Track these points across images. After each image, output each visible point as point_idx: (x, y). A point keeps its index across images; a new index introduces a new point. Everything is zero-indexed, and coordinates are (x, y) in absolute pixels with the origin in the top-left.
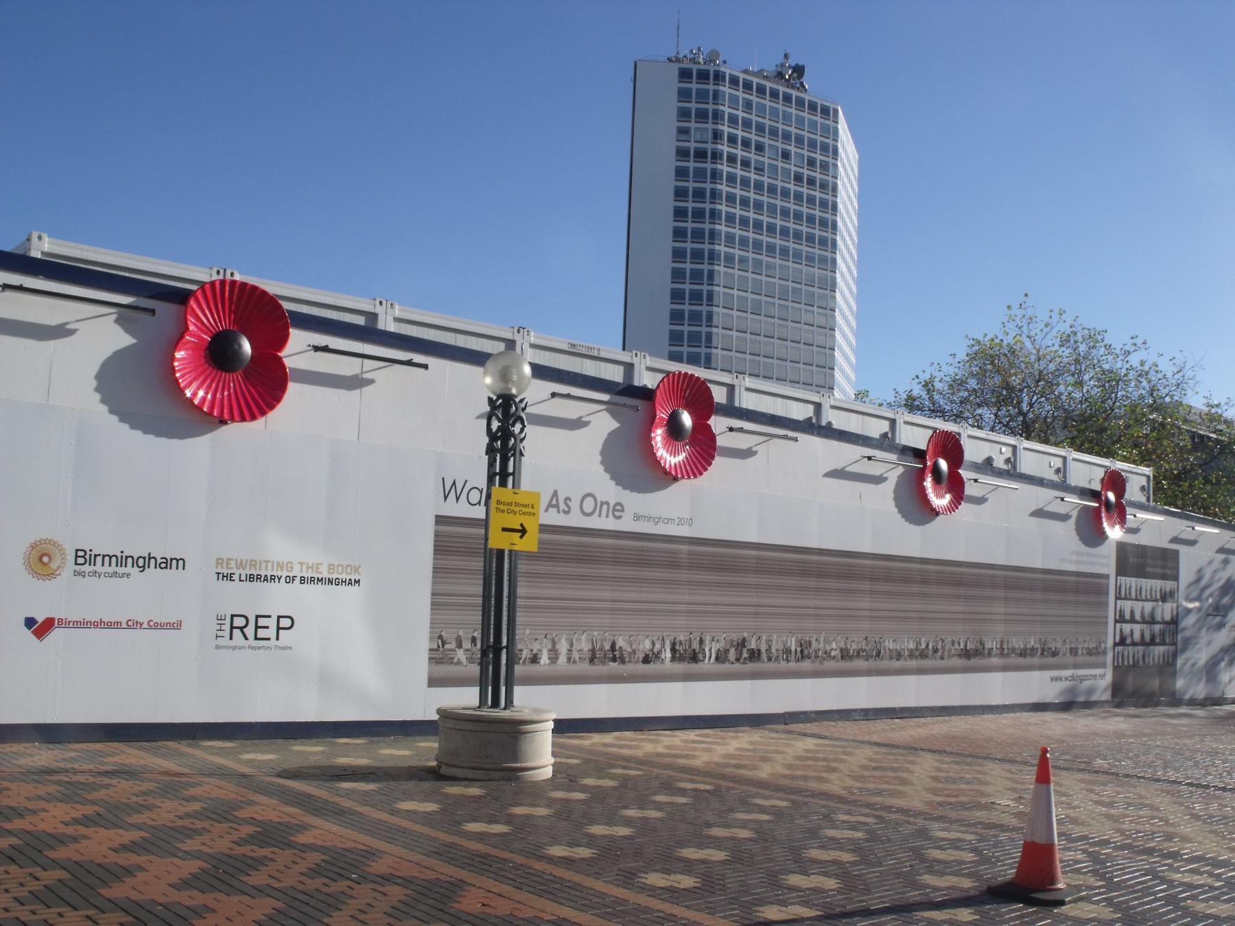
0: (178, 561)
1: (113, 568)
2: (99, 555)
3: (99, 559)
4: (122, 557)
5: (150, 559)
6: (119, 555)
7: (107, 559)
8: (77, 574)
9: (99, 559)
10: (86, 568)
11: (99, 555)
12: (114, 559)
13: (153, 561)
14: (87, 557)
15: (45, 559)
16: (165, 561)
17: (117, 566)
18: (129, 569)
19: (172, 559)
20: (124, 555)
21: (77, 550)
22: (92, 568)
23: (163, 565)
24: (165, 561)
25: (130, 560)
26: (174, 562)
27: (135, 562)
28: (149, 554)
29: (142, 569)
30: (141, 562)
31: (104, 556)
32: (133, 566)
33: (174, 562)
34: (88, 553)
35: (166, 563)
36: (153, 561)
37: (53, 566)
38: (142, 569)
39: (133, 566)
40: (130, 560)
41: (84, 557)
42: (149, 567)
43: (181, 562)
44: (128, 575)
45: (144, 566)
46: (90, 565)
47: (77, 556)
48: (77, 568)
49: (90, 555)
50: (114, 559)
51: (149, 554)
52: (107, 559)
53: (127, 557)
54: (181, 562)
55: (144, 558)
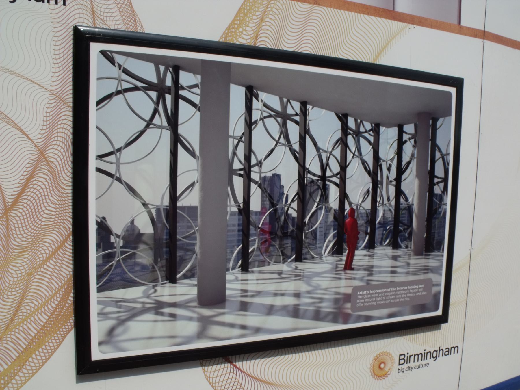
3: (412, 358)
4: (425, 353)
5: (440, 350)
11: (412, 355)
12: (420, 356)
14: (406, 358)
17: (422, 360)
27: (432, 356)
28: (440, 348)
29: (435, 358)
31: (415, 355)
34: (406, 355)
36: (441, 352)
42: (439, 357)
45: (436, 357)
47: (400, 359)
49: (407, 356)
50: (420, 356)
51: (440, 348)
52: (416, 357)
55: (437, 351)
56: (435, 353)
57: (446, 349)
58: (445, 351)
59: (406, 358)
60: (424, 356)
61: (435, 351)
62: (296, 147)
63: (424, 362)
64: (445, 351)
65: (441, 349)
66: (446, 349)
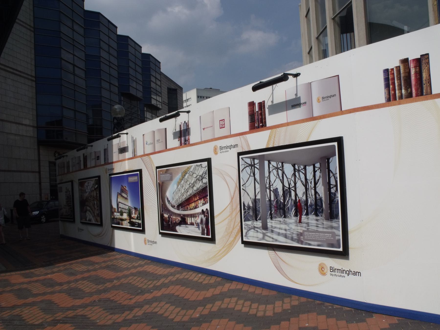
1: (340, 274)
2: (336, 269)
3: (336, 270)
5: (350, 271)
6: (341, 269)
8: (331, 275)
9: (336, 270)
10: (333, 273)
11: (336, 269)
12: (340, 270)
13: (351, 272)
14: (333, 269)
15: (323, 269)
16: (354, 272)
17: (341, 273)
18: (344, 275)
19: (357, 272)
20: (343, 269)
21: (330, 267)
23: (354, 274)
24: (354, 272)
25: (344, 271)
26: (357, 273)
27: (346, 273)
28: (350, 270)
29: (348, 275)
31: (337, 269)
32: (345, 274)
33: (357, 273)
34: (333, 268)
35: (355, 273)
36: (351, 272)
37: (325, 271)
38: (348, 275)
39: (345, 274)
40: (344, 271)
42: (350, 274)
43: (359, 273)
44: (344, 277)
45: (348, 274)
46: (334, 272)
47: (330, 269)
50: (340, 270)
51: (350, 270)
52: (338, 270)
53: (343, 270)
54: (359, 273)
55: (348, 271)
56: (347, 272)
57: (354, 271)
58: (353, 272)
59: (333, 269)
60: (342, 271)
61: (347, 271)
62: (281, 178)
63: (342, 275)
64: (353, 272)
65: (350, 270)
66: (354, 271)
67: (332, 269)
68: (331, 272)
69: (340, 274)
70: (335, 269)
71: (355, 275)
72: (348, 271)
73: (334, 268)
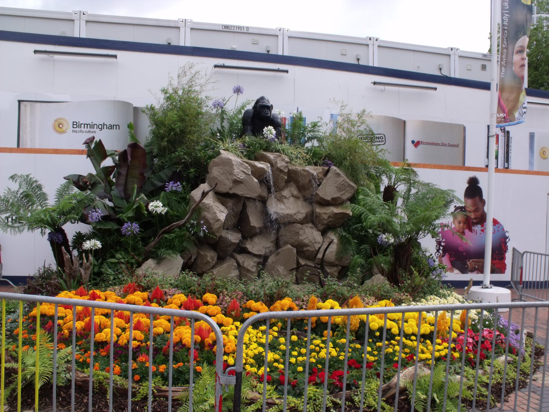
0: (116, 126)
1: (89, 129)
3: (83, 126)
5: (104, 125)
7: (86, 125)
8: (73, 131)
9: (83, 126)
10: (77, 129)
12: (89, 125)
13: (105, 126)
14: (78, 125)
15: (61, 126)
18: (95, 129)
20: (93, 124)
22: (80, 129)
25: (95, 126)
27: (98, 127)
30: (100, 127)
31: (84, 124)
34: (78, 123)
37: (64, 128)
41: (76, 125)
43: (118, 127)
45: (102, 128)
47: (73, 125)
48: (74, 129)
52: (86, 125)
53: (94, 125)
55: (102, 125)
58: (108, 126)
64: (108, 126)
67: (76, 125)
68: (73, 127)
69: (89, 129)
70: (81, 124)
71: (111, 129)
72: (102, 125)
73: (80, 123)
